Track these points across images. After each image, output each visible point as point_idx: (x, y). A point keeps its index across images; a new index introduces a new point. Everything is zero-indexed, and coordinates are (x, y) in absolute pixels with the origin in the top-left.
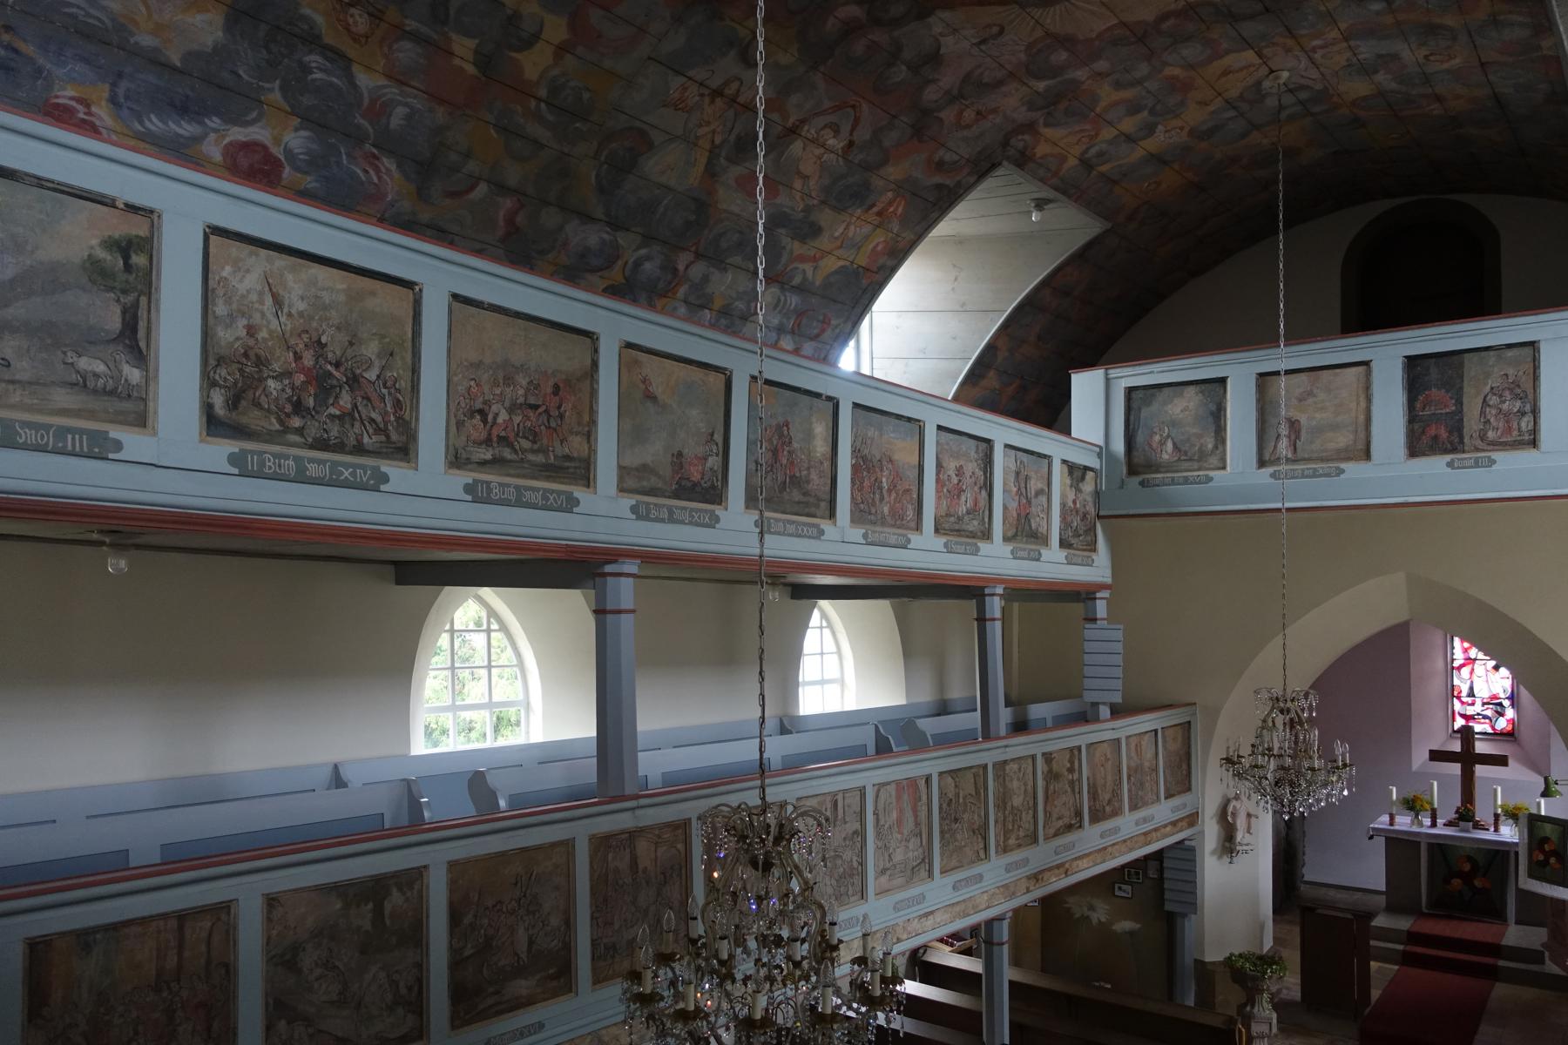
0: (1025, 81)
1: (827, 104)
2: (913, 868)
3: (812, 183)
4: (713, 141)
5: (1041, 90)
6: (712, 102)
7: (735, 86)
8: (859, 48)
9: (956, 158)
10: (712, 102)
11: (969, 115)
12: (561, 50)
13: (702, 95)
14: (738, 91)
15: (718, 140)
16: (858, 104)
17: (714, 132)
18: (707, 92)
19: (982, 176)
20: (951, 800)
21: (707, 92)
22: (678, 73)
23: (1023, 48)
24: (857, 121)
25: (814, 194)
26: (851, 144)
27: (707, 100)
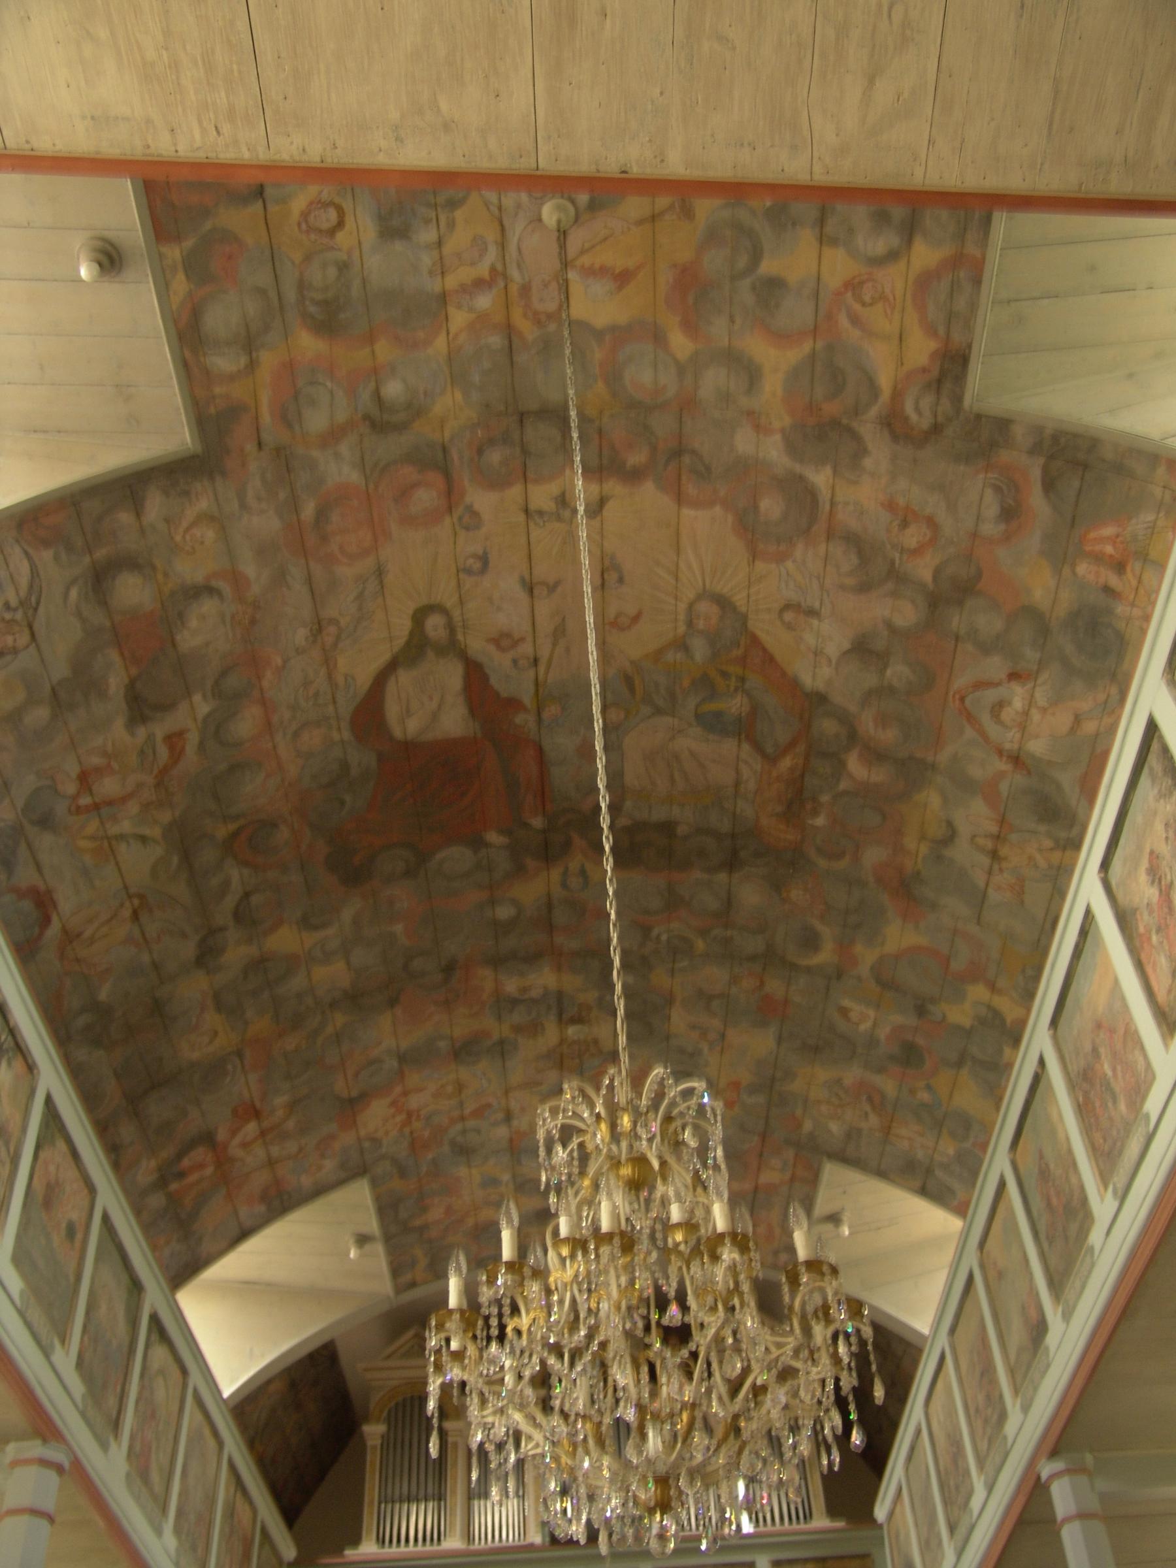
0: (827, 507)
1: (969, 733)
3: (1085, 705)
4: (1051, 849)
5: (828, 470)
7: (981, 841)
8: (888, 736)
9: (989, 494)
11: (913, 537)
13: (1001, 870)
15: (1048, 843)
16: (957, 696)
17: (1040, 850)
19: (1003, 424)
21: (996, 867)
23: (789, 564)
24: (980, 685)
25: (1102, 697)
26: (1014, 676)
27: (1004, 865)
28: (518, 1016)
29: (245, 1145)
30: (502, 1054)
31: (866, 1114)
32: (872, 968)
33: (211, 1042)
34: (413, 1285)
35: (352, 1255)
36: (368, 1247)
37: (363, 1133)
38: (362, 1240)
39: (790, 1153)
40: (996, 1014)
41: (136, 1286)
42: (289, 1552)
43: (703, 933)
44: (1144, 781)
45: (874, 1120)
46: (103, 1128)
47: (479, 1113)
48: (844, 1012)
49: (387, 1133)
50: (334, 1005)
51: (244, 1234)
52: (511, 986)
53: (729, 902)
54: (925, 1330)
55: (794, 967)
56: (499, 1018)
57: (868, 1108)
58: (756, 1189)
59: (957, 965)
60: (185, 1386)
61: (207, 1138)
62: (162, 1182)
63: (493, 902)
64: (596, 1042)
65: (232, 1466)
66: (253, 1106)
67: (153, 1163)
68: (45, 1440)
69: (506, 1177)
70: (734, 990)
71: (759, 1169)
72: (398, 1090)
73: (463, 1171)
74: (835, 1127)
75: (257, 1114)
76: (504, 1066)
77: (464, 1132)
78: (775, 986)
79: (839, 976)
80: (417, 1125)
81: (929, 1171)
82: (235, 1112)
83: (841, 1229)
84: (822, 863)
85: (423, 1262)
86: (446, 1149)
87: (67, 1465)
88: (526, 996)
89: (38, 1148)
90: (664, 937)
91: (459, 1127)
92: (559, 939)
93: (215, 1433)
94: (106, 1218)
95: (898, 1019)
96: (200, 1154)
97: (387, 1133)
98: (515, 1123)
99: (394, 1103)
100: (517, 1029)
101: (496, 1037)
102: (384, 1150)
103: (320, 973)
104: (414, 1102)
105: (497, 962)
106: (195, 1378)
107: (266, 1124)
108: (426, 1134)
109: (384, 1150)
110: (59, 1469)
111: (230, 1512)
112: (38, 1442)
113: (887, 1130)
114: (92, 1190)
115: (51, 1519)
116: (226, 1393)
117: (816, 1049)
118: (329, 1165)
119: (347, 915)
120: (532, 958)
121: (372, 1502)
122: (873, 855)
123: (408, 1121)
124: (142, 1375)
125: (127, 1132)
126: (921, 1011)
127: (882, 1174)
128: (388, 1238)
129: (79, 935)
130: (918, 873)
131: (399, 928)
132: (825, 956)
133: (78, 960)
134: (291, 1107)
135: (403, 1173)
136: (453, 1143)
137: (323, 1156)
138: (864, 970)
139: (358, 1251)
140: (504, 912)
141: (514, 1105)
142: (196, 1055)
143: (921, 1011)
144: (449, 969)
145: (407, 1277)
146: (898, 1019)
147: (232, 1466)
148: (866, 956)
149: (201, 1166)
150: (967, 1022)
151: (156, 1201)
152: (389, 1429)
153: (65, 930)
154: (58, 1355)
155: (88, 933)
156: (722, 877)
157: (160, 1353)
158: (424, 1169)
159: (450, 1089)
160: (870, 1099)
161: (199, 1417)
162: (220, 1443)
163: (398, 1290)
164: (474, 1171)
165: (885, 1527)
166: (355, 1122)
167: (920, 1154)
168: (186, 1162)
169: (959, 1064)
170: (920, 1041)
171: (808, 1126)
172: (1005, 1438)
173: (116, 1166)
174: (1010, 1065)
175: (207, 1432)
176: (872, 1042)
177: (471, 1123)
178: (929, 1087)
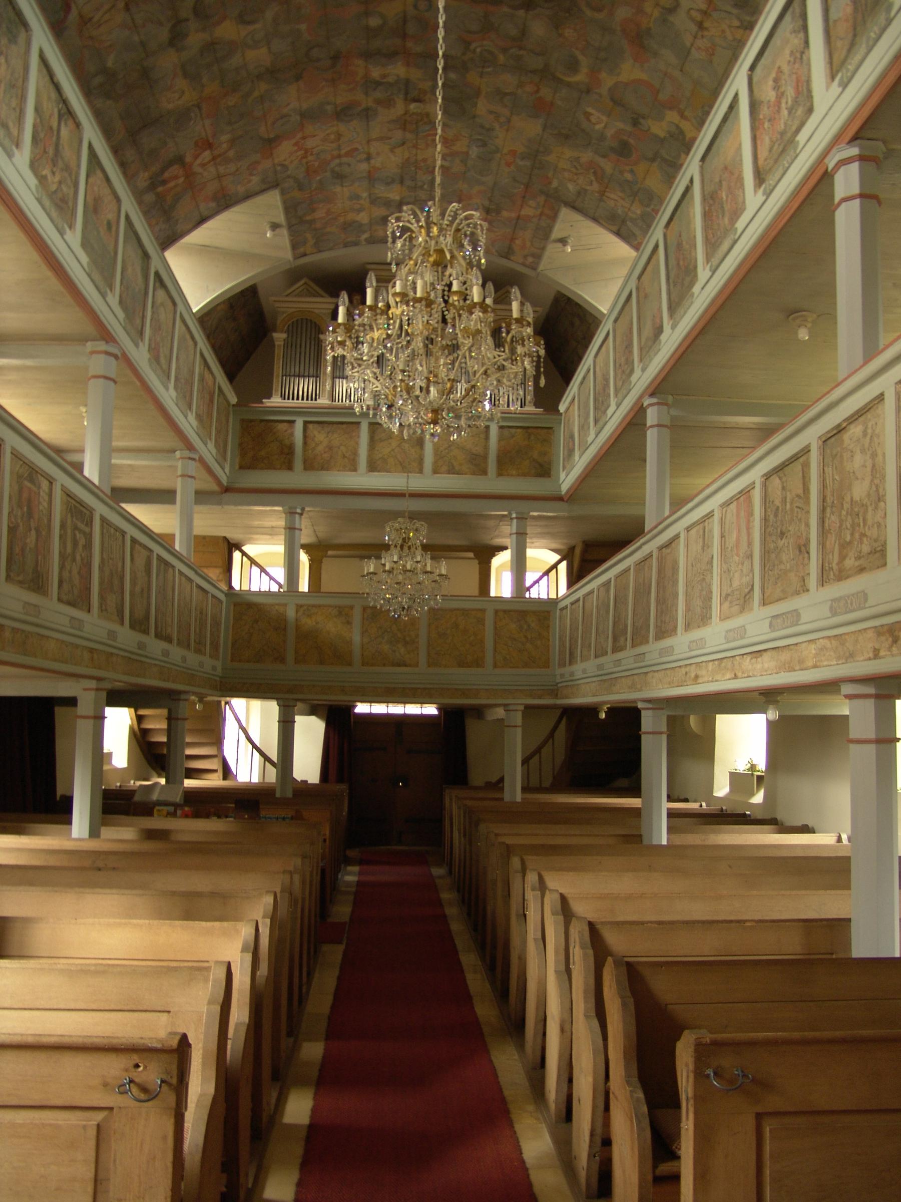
2: (745, 596)
4: (738, 27)
6: (706, 29)
7: (694, 14)
10: (706, 29)
12: (682, 116)
13: (703, 36)
14: (698, 10)
15: (736, 23)
17: (730, 27)
18: (700, 33)
20: (778, 508)
22: (689, 52)
27: (706, 33)
28: (379, 94)
29: (203, 165)
30: (367, 117)
31: (592, 181)
32: (609, 89)
33: (180, 98)
34: (305, 255)
35: (268, 235)
36: (278, 230)
37: (276, 161)
38: (275, 226)
39: (542, 199)
40: (682, 132)
41: (146, 256)
42: (234, 400)
43: (504, 50)
44: (788, 17)
45: (596, 186)
46: (116, 151)
47: (349, 154)
48: (587, 115)
49: (291, 162)
50: (259, 77)
51: (202, 221)
52: (376, 73)
53: (524, 32)
54: (605, 312)
55: (560, 81)
56: (366, 94)
57: (593, 178)
58: (518, 218)
59: (661, 97)
60: (175, 313)
61: (179, 160)
62: (152, 187)
63: (367, 14)
64: (428, 115)
65: (202, 355)
66: (208, 140)
67: (147, 174)
68: (107, 342)
69: (365, 195)
70: (520, 91)
71: (522, 206)
72: (300, 135)
73: (338, 189)
74: (571, 186)
75: (210, 146)
76: (368, 125)
77: (340, 165)
78: (546, 92)
79: (588, 91)
80: (310, 158)
81: (624, 222)
82: (196, 144)
83: (566, 248)
84: (589, 13)
85: (311, 242)
86: (328, 174)
87: (119, 354)
88: (385, 80)
89: (88, 176)
90: (478, 50)
91: (337, 161)
92: (409, 44)
93: (193, 338)
94: (127, 217)
95: (620, 125)
96: (175, 170)
97: (291, 162)
98: (373, 161)
99: (296, 144)
100: (379, 102)
101: (364, 106)
102: (289, 172)
103: (251, 54)
104: (310, 143)
105: (367, 56)
106: (181, 307)
107: (216, 153)
108: (317, 164)
109: (289, 172)
110: (116, 357)
111: (202, 379)
112: (104, 342)
113: (602, 193)
114: (118, 200)
115: (115, 382)
116: (194, 311)
117: (567, 137)
118: (255, 179)
119: (269, 14)
120: (391, 55)
121: (278, 376)
122: (623, 13)
123: (305, 157)
124: (153, 307)
125: (130, 154)
126: (635, 123)
127: (595, 220)
128: (290, 227)
129: (91, 19)
130: (649, 29)
131: (303, 27)
132: (580, 77)
133: (91, 38)
134: (232, 142)
135: (301, 187)
136: (333, 171)
137: (251, 175)
138: (604, 90)
139: (272, 233)
140: (374, 22)
141: (373, 150)
142: (171, 106)
143: (635, 123)
144: (336, 58)
145: (302, 250)
146: (620, 125)
147: (202, 355)
148: (607, 81)
149: (176, 177)
150: (662, 134)
151: (150, 198)
152: (288, 337)
153: (81, 16)
154: (110, 298)
155: (95, 19)
156: (521, 13)
157: (161, 293)
158: (314, 186)
159: (332, 137)
160: (595, 173)
161: (184, 328)
162: (195, 343)
163: (296, 258)
164: (345, 189)
165: (563, 415)
166: (272, 154)
167: (620, 211)
168: (167, 175)
169: (653, 160)
170: (631, 141)
171: (555, 184)
172: (631, 382)
173: (125, 174)
174: (682, 165)
175: (188, 337)
176: (602, 137)
177: (344, 160)
178: (632, 171)
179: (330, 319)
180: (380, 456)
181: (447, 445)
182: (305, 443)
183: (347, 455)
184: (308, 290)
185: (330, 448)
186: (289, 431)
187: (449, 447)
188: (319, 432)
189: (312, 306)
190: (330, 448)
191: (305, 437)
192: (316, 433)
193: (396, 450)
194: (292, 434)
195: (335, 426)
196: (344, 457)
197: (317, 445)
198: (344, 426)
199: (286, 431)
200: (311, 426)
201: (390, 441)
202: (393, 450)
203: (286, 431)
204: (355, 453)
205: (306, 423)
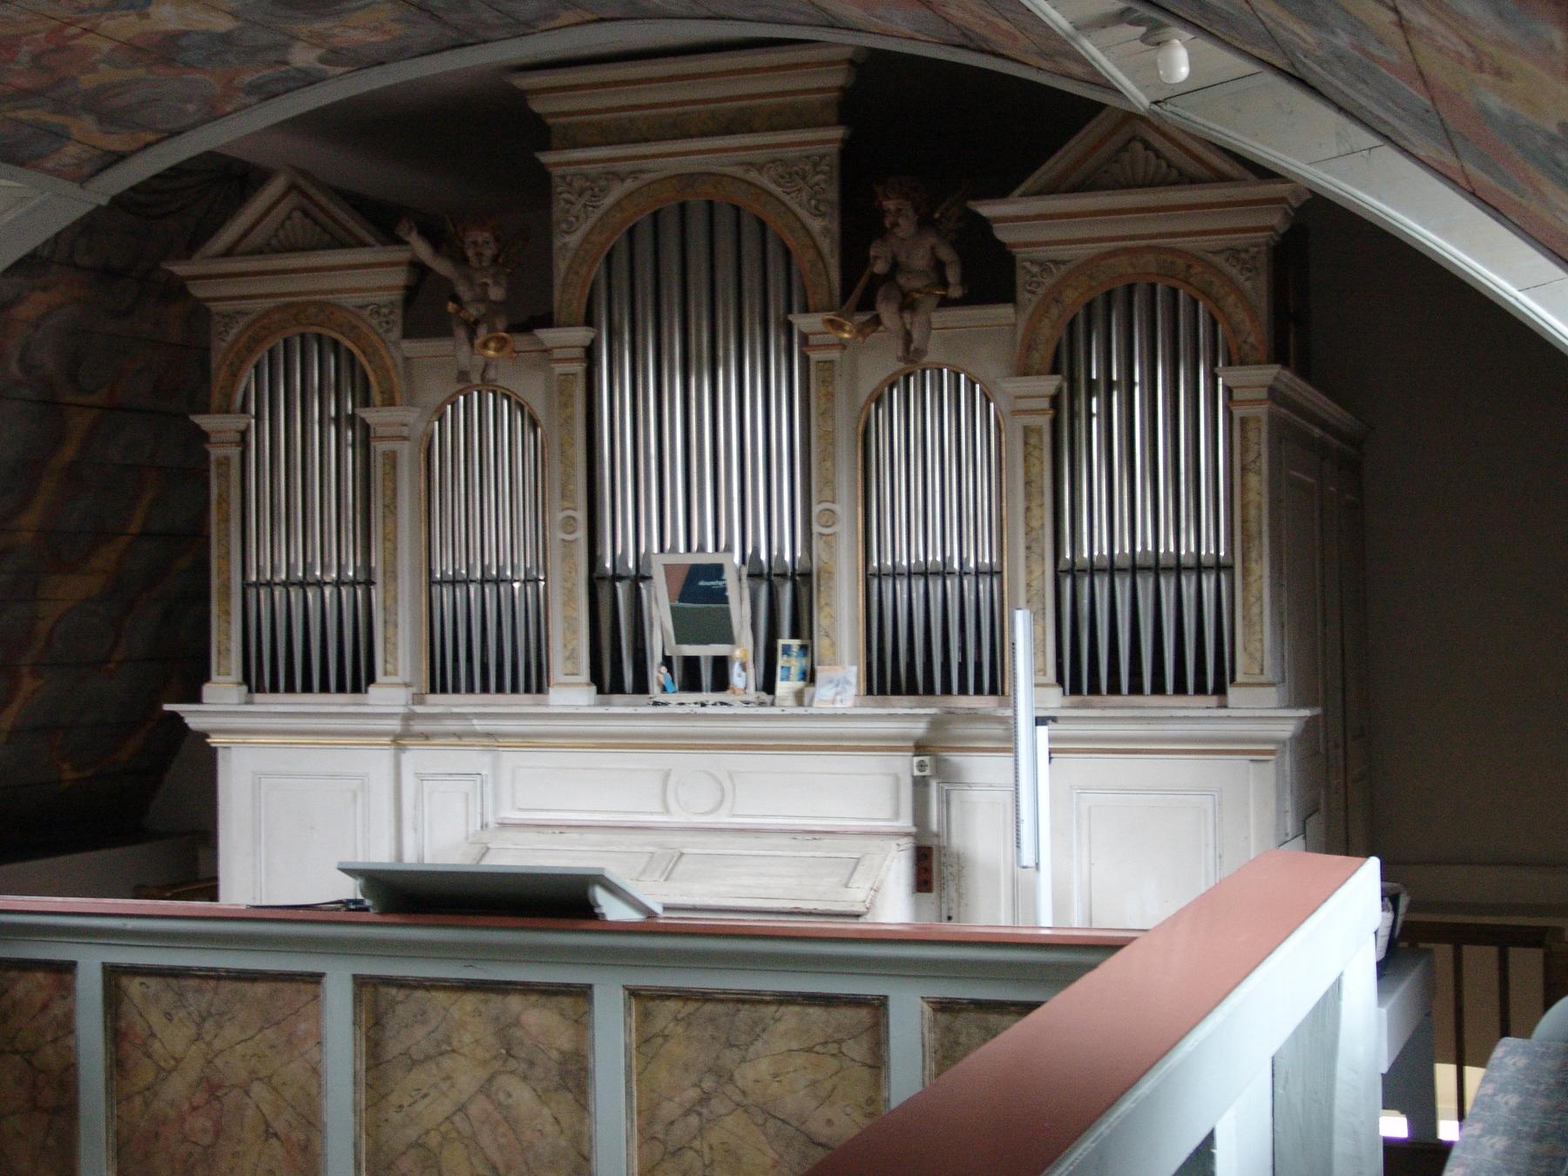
121: (226, 586)
179: (396, 333)
180: (412, 1133)
181: (693, 1093)
182: (117, 1066)
183: (279, 1126)
184: (306, 213)
185: (212, 1088)
186: (58, 1010)
187: (705, 1099)
188: (169, 1016)
189: (327, 282)
190: (212, 1088)
191: (116, 1035)
192: (155, 1018)
193: (473, 1110)
194: (67, 1025)
195: (227, 987)
196: (269, 1133)
197: (163, 1074)
198: (261, 989)
199: (45, 1007)
200: (134, 986)
201: (447, 1063)
202: (462, 1108)
203: (45, 1007)
204: (311, 1120)
205: (113, 974)
